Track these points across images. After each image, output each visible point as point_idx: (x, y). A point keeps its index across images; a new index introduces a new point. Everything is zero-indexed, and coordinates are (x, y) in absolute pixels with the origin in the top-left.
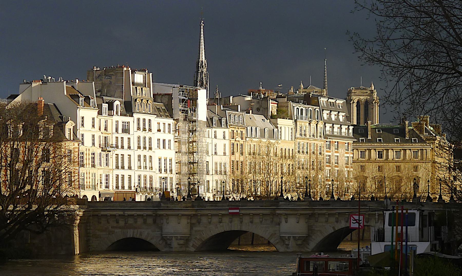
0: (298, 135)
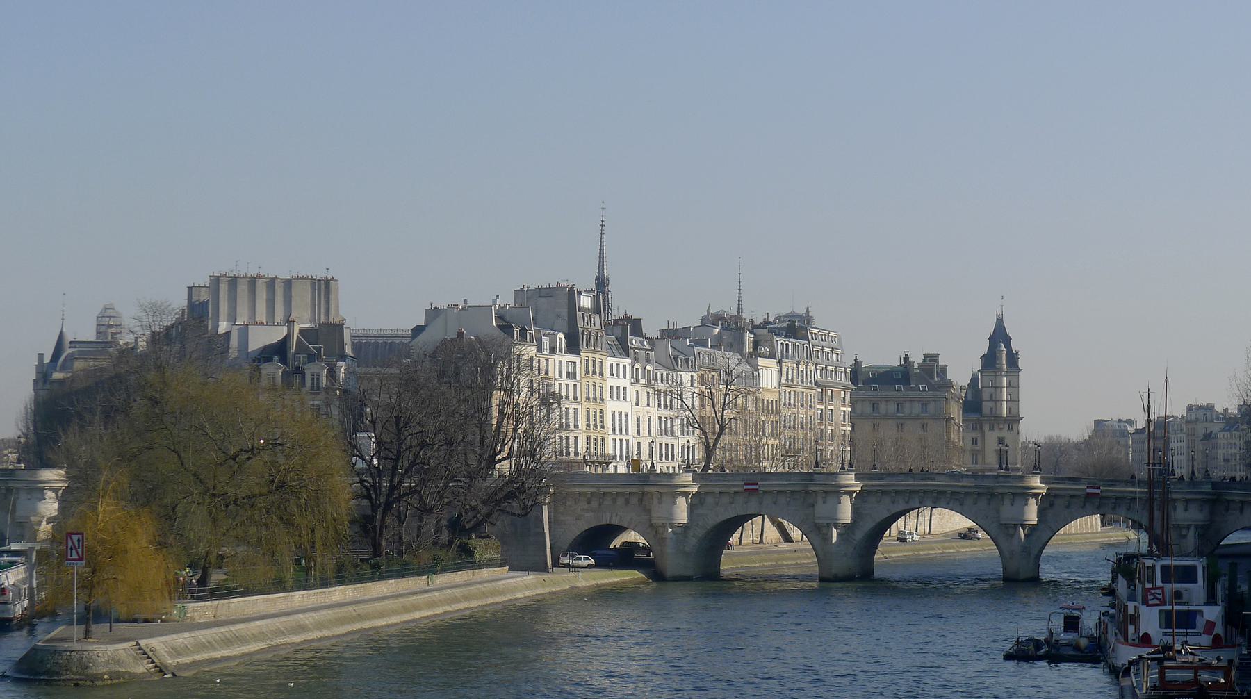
0: (783, 381)
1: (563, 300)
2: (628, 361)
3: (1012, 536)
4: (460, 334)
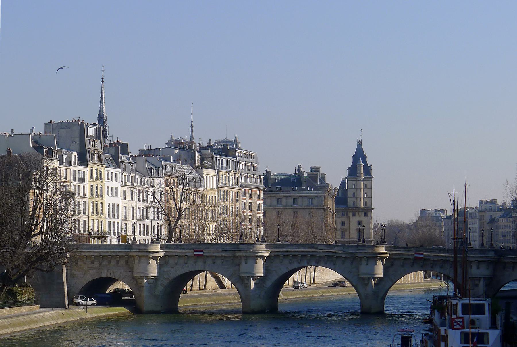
0: (220, 184)
1: (77, 131)
2: (118, 171)
3: (367, 285)
4: (9, 152)
